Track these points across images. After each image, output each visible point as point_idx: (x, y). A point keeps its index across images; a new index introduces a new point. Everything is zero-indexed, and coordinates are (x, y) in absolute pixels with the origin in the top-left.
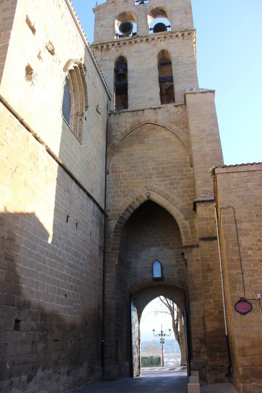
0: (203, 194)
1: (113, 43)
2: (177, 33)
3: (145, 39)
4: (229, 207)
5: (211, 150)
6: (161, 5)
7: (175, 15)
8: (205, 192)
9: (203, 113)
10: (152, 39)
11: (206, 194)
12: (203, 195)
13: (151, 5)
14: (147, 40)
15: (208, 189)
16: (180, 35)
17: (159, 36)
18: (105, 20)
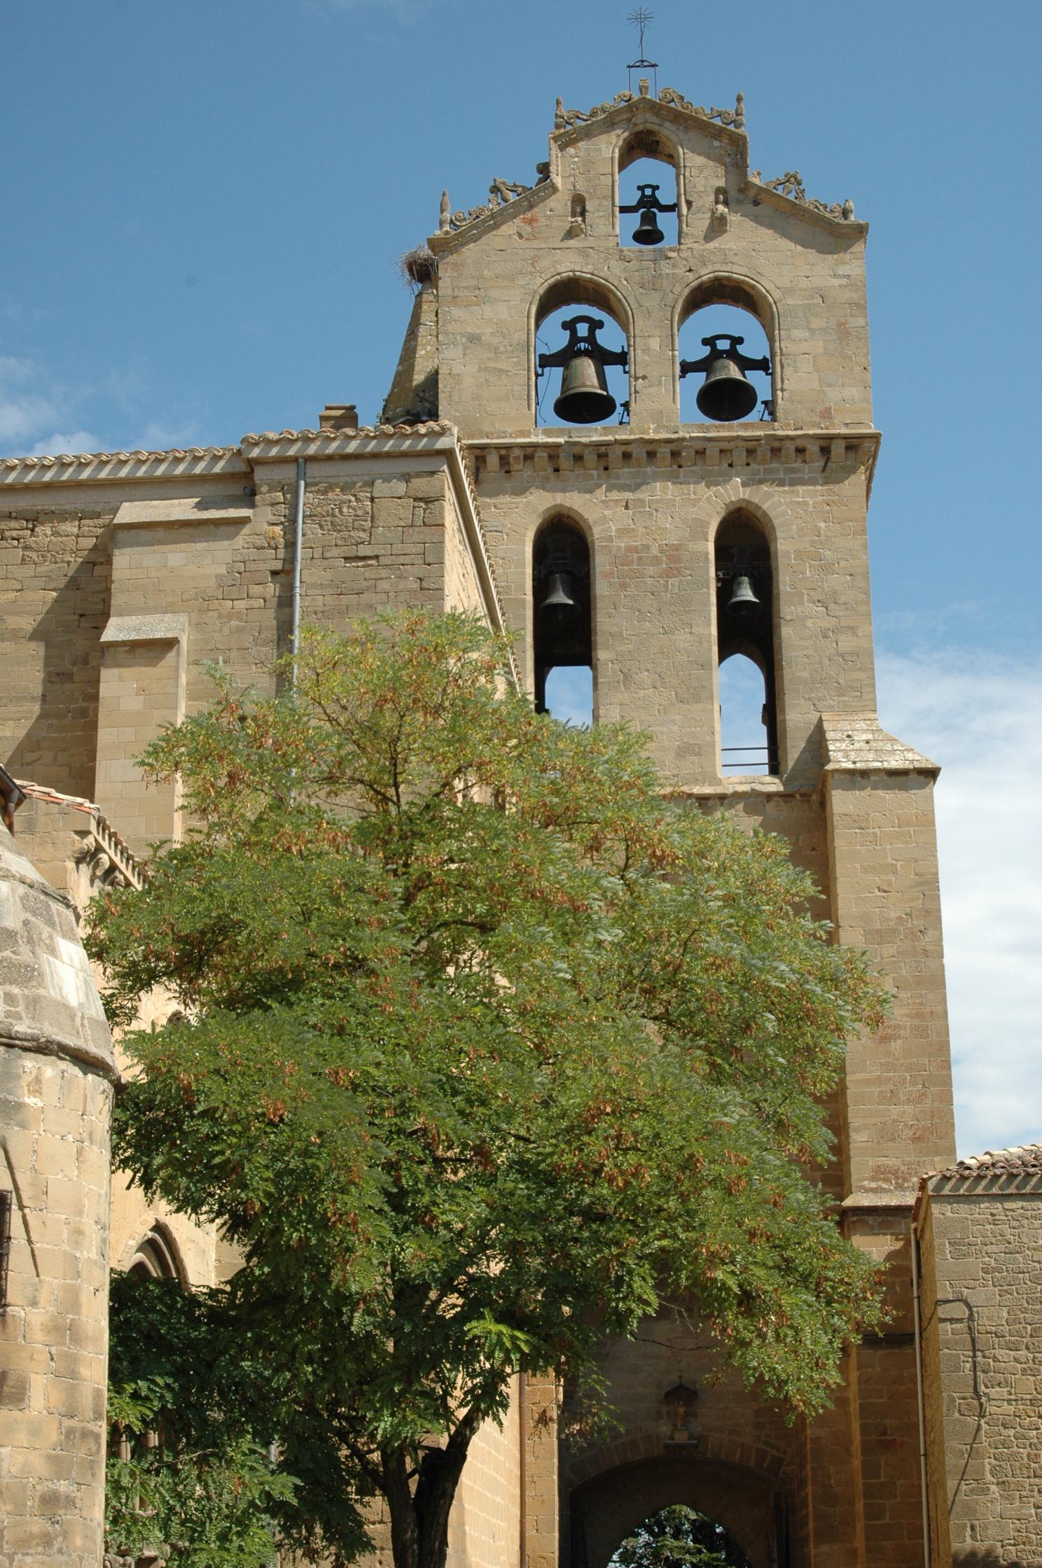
0: (873, 1179)
1: (529, 450)
2: (800, 443)
3: (664, 451)
4: (961, 1300)
5: (908, 1016)
6: (738, 271)
7: (797, 334)
8: (880, 1173)
9: (890, 861)
10: (697, 452)
11: (885, 1180)
12: (873, 1185)
13: (692, 263)
14: (675, 454)
15: (892, 1162)
16: (813, 448)
17: (725, 445)
18: (487, 310)
